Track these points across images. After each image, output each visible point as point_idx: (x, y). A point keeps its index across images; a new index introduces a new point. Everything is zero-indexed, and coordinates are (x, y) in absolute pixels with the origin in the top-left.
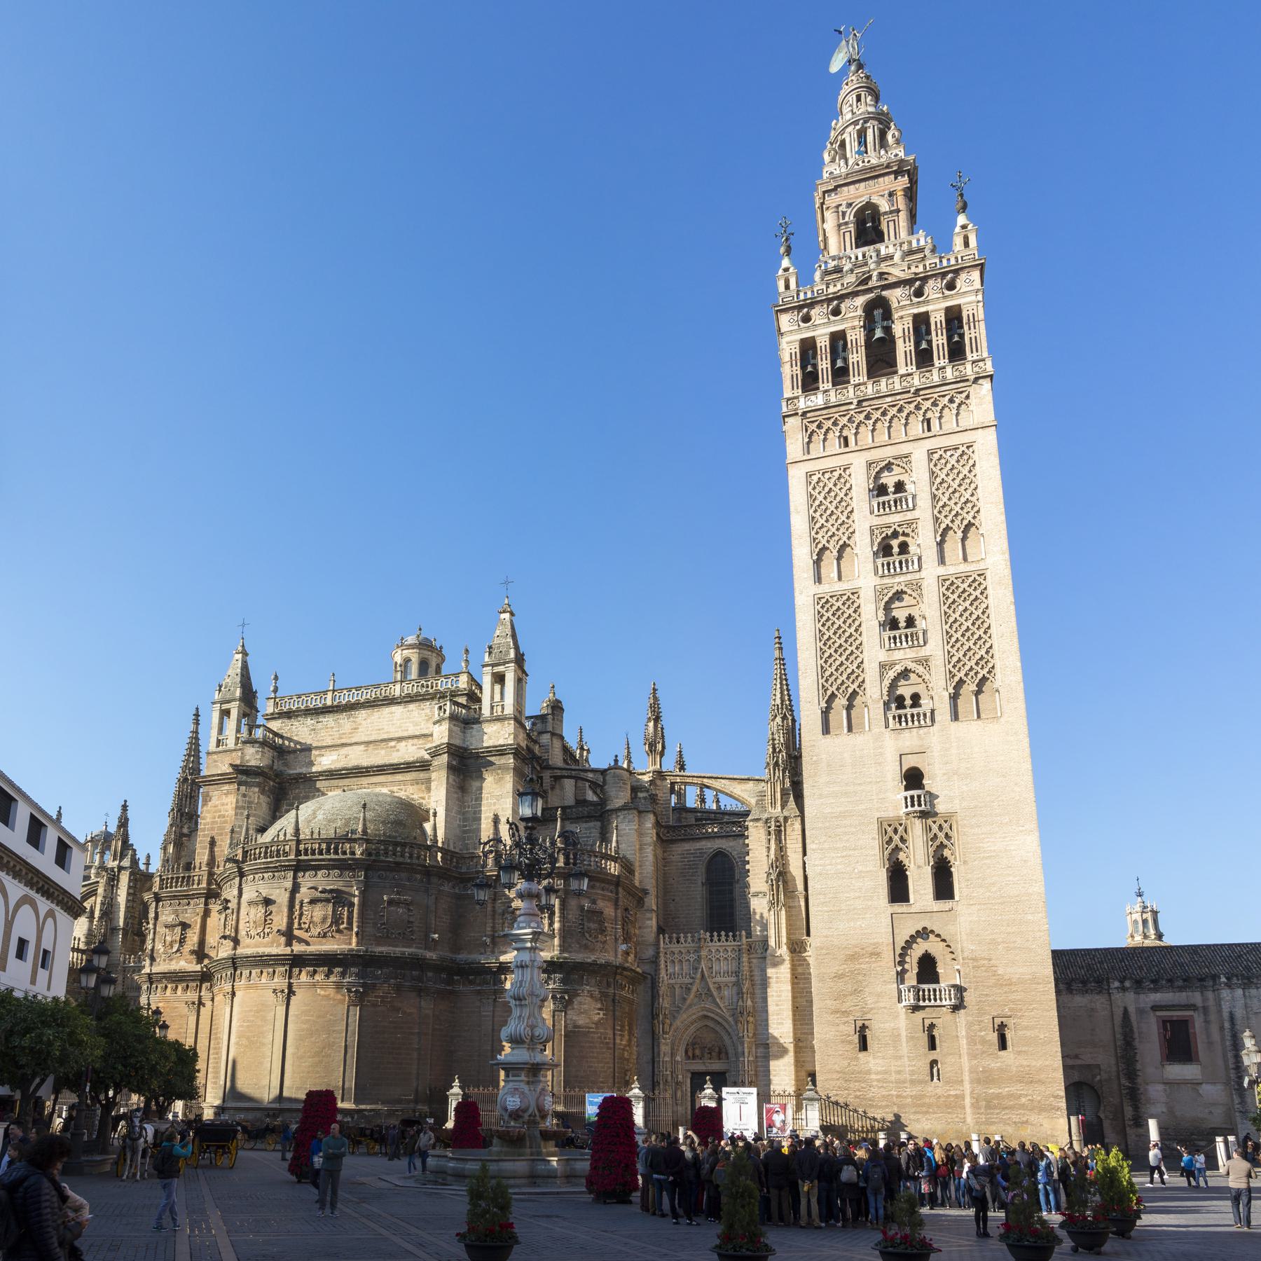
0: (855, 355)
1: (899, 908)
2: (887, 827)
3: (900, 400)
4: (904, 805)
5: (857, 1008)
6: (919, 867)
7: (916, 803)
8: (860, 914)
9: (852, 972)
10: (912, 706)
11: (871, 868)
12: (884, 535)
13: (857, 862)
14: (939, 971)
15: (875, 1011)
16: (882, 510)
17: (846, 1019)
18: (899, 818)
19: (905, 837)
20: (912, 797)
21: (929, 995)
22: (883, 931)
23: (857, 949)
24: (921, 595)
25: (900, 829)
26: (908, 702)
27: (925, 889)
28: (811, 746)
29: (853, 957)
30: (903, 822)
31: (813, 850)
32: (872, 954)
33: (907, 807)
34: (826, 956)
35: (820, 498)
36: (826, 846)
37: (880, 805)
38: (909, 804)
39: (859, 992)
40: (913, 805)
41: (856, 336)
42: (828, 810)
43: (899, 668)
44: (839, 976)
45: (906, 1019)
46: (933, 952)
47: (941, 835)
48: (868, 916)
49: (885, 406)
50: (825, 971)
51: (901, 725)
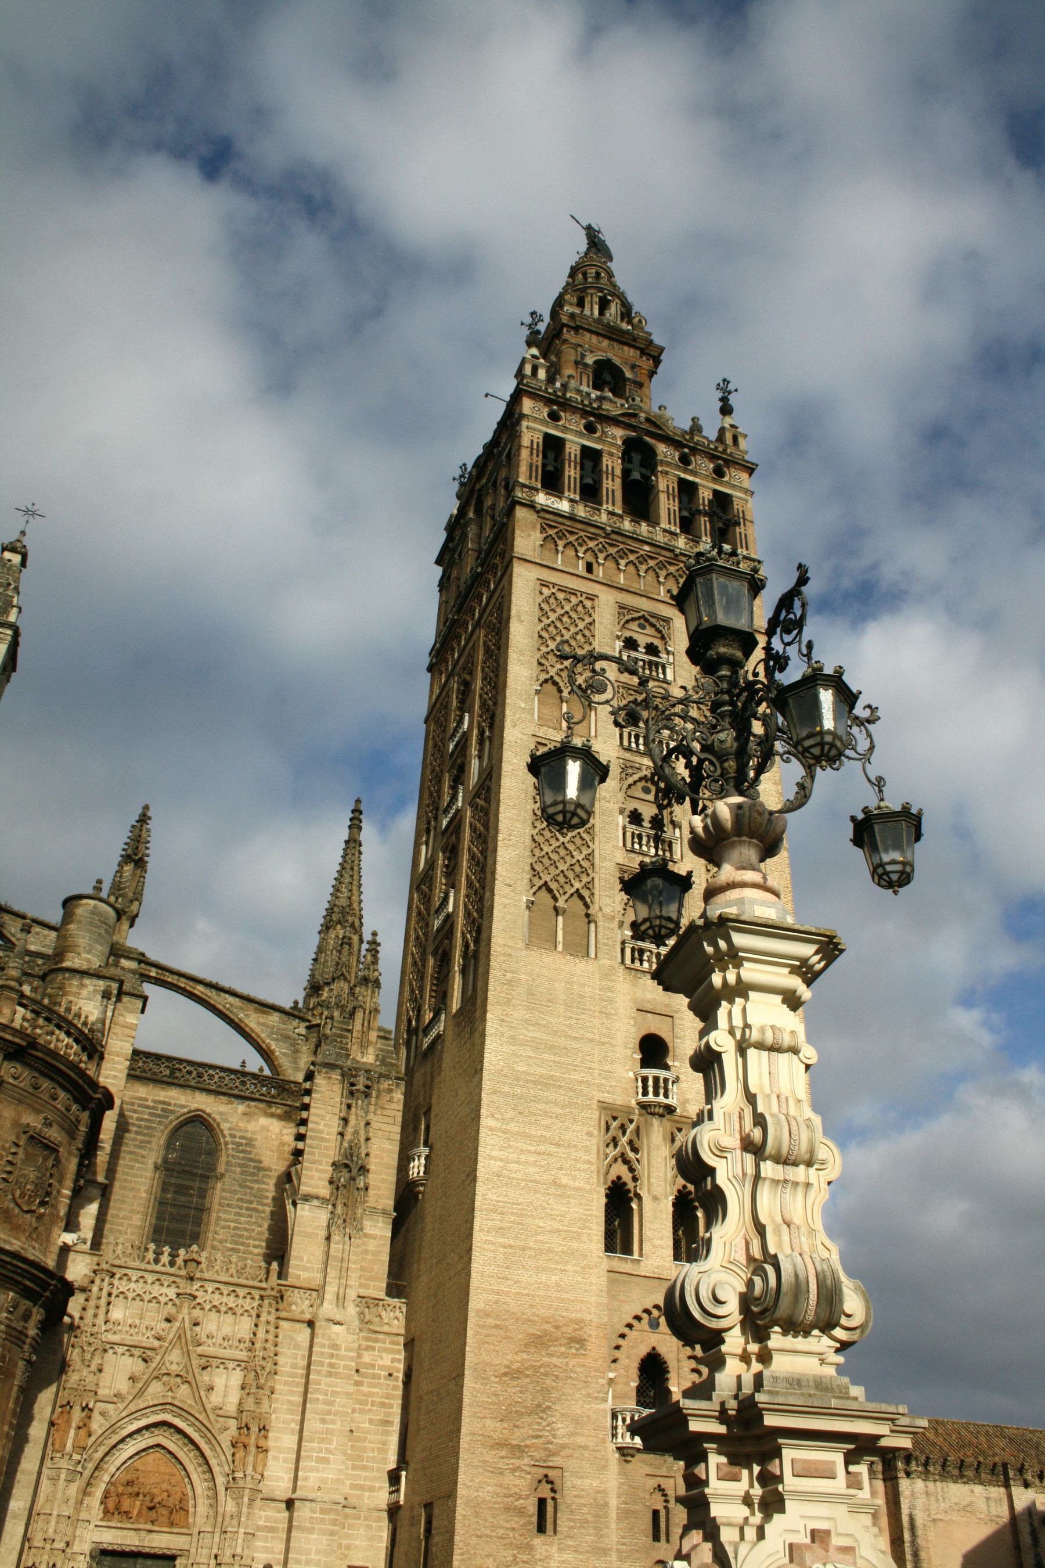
1: (619, 1262)
2: (611, 1121)
3: (659, 554)
5: (541, 1441)
6: (655, 1198)
7: (662, 1091)
8: (557, 1263)
9: (536, 1369)
11: (582, 1184)
12: (632, 698)
13: (561, 1168)
15: (568, 1451)
17: (517, 1462)
18: (629, 1110)
19: (635, 1140)
20: (656, 1079)
22: (594, 1298)
23: (547, 1327)
25: (632, 1127)
27: (661, 1238)
28: (504, 955)
29: (539, 1341)
30: (635, 1118)
31: (491, 1129)
32: (573, 1340)
33: (645, 1093)
34: (494, 1331)
35: (553, 617)
36: (512, 1127)
37: (603, 1081)
38: (640, 1090)
39: (543, 1411)
40: (656, 1094)
41: (612, 463)
42: (522, 1067)
44: (512, 1374)
45: (620, 1473)
46: (662, 1350)
48: (569, 1267)
49: (642, 552)
50: (487, 1359)
51: (641, 964)
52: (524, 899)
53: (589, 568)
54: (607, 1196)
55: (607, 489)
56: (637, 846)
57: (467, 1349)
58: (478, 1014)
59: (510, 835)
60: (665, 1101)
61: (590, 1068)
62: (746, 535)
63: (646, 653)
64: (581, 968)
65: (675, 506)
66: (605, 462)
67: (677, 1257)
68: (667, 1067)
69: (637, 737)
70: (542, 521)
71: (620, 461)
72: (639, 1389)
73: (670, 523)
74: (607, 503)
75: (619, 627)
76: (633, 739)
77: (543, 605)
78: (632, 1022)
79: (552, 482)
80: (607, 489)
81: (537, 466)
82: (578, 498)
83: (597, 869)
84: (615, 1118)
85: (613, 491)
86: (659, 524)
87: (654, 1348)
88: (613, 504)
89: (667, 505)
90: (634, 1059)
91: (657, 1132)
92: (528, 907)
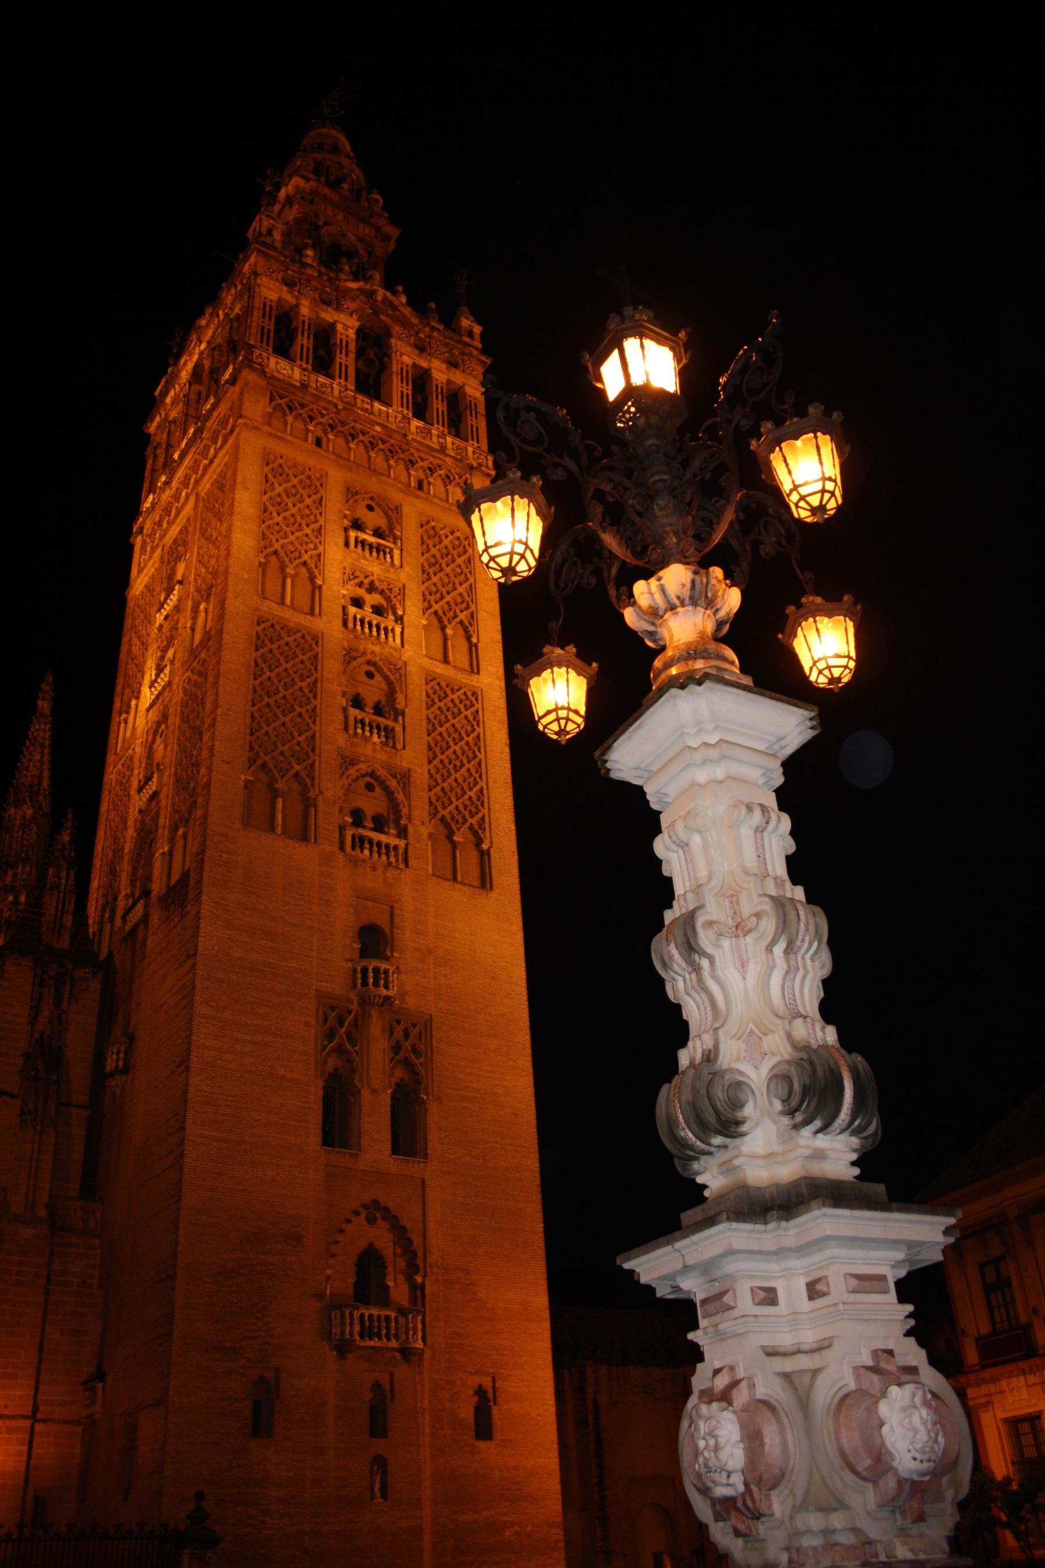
0: (343, 356)
4: (359, 981)
6: (374, 1091)
10: (374, 830)
14: (391, 1284)
16: (360, 547)
20: (376, 971)
21: (379, 1328)
24: (400, 681)
26: (369, 824)
43: (362, 767)
47: (407, 1045)
49: (373, 433)
51: (362, 852)
52: (243, 777)
53: (318, 443)
54: (324, 1088)
55: (341, 364)
56: (359, 731)
57: (179, 1248)
58: (190, 896)
59: (229, 710)
60: (385, 992)
61: (308, 956)
62: (477, 428)
63: (374, 535)
64: (301, 851)
65: (409, 390)
66: (339, 336)
67: (395, 1150)
68: (387, 959)
69: (362, 621)
70: (270, 387)
71: (354, 337)
72: (355, 1284)
73: (402, 406)
74: (340, 377)
75: (347, 506)
76: (359, 623)
77: (269, 475)
78: (352, 910)
79: (283, 350)
80: (341, 364)
81: (269, 330)
82: (310, 367)
83: (317, 752)
84: (333, 1008)
85: (346, 366)
86: (391, 406)
87: (371, 1244)
88: (346, 380)
89: (399, 387)
90: (353, 949)
91: (376, 1026)
92: (246, 787)
